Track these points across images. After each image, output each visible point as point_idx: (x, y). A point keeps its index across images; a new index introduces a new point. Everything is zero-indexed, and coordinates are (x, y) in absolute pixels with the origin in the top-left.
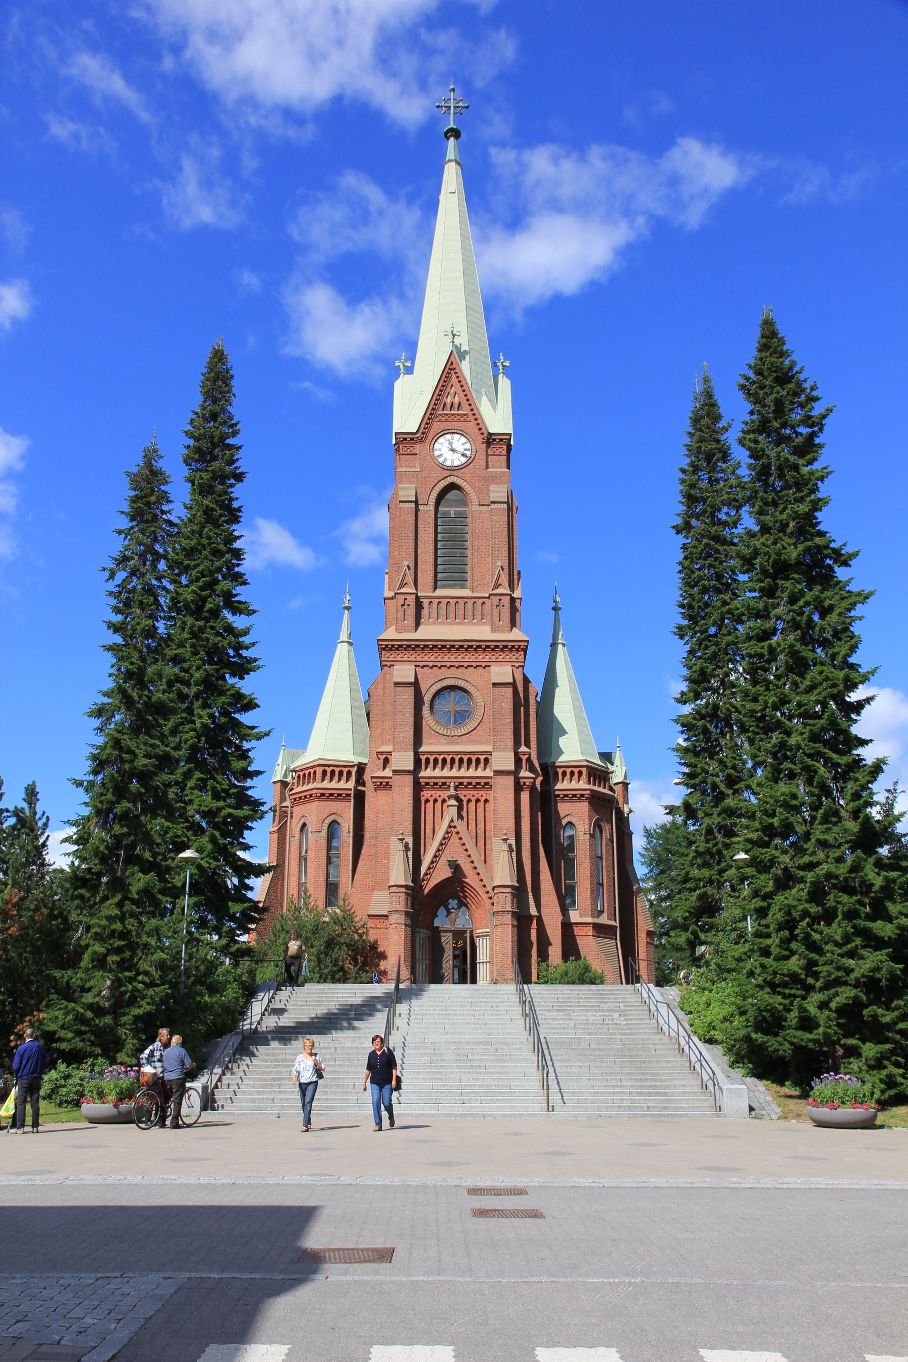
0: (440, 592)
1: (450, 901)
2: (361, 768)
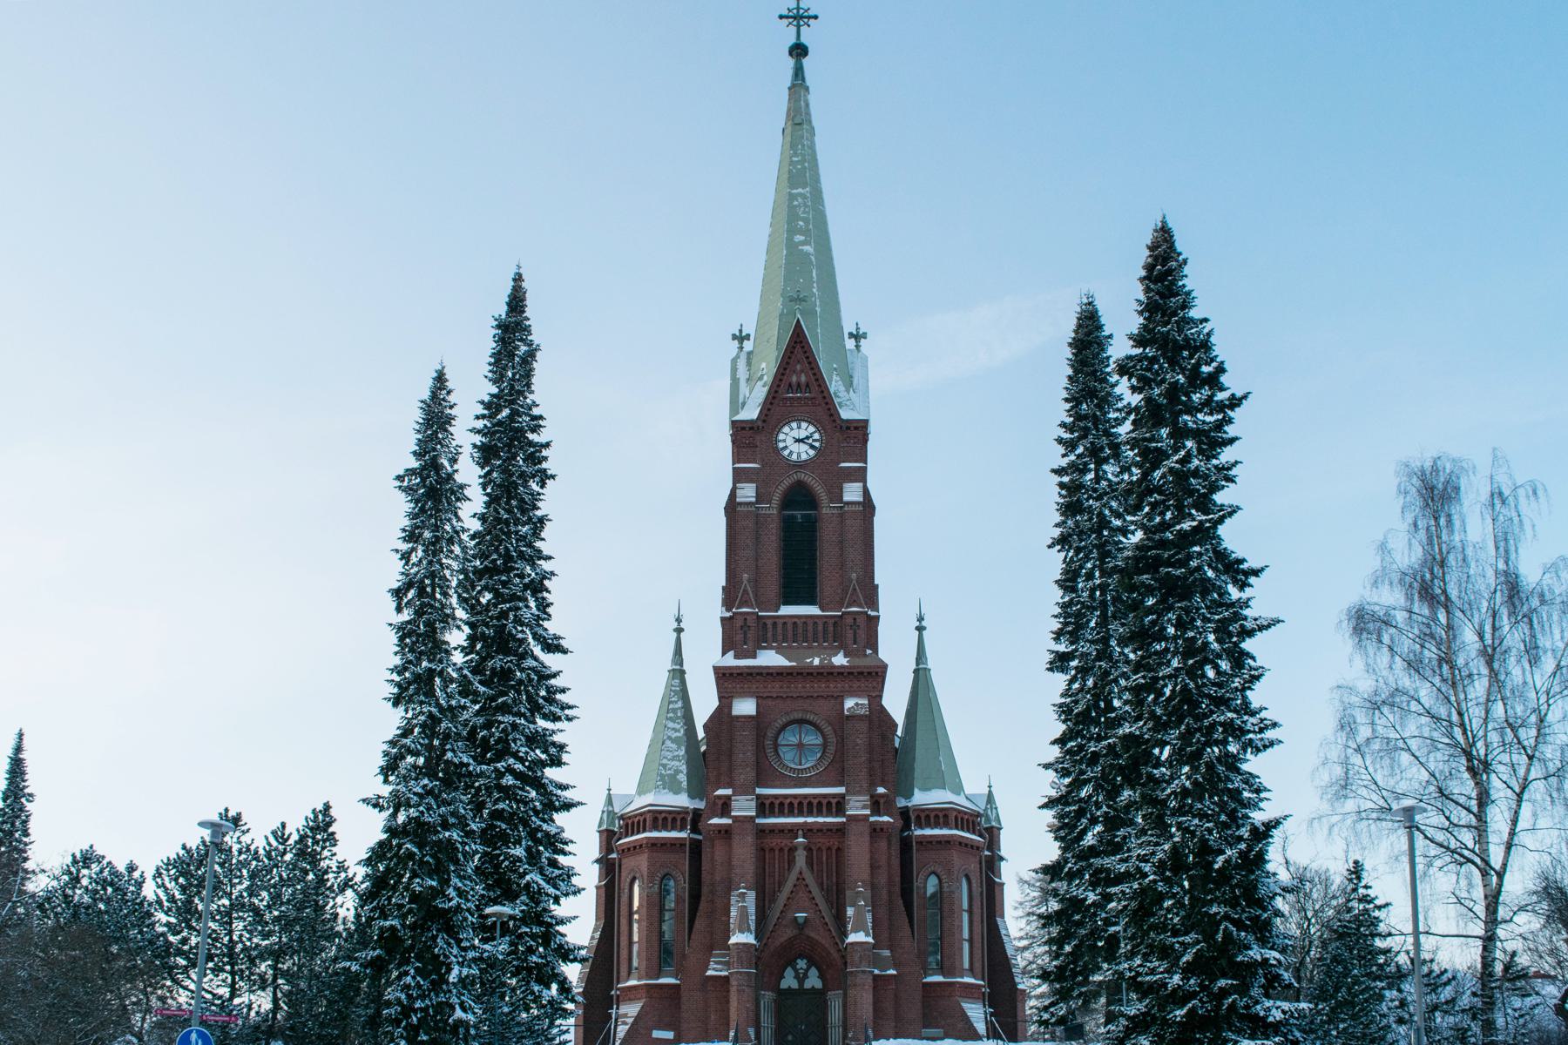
0: (786, 610)
1: (799, 961)
2: (697, 814)
